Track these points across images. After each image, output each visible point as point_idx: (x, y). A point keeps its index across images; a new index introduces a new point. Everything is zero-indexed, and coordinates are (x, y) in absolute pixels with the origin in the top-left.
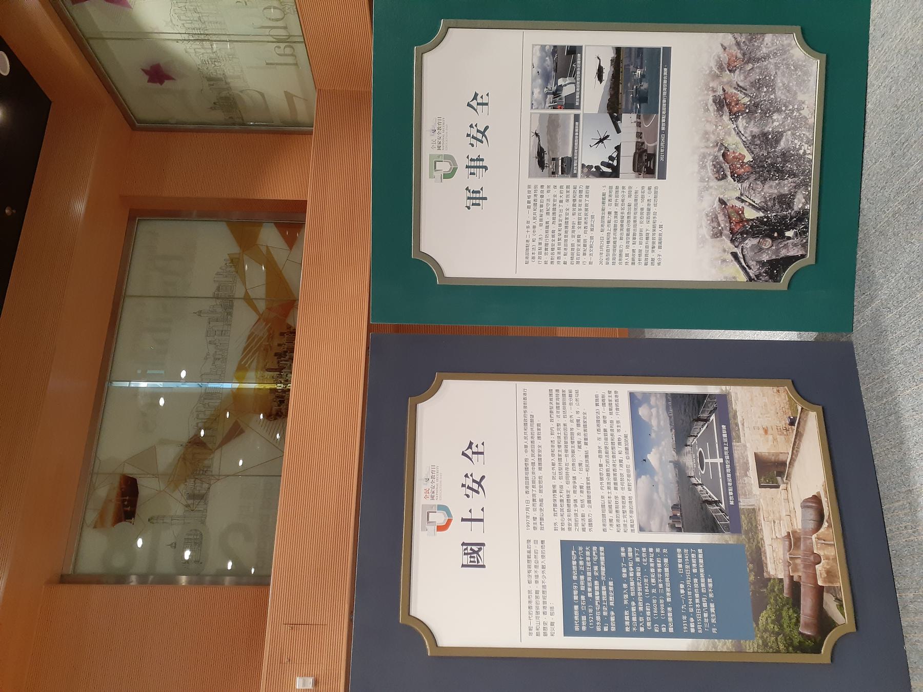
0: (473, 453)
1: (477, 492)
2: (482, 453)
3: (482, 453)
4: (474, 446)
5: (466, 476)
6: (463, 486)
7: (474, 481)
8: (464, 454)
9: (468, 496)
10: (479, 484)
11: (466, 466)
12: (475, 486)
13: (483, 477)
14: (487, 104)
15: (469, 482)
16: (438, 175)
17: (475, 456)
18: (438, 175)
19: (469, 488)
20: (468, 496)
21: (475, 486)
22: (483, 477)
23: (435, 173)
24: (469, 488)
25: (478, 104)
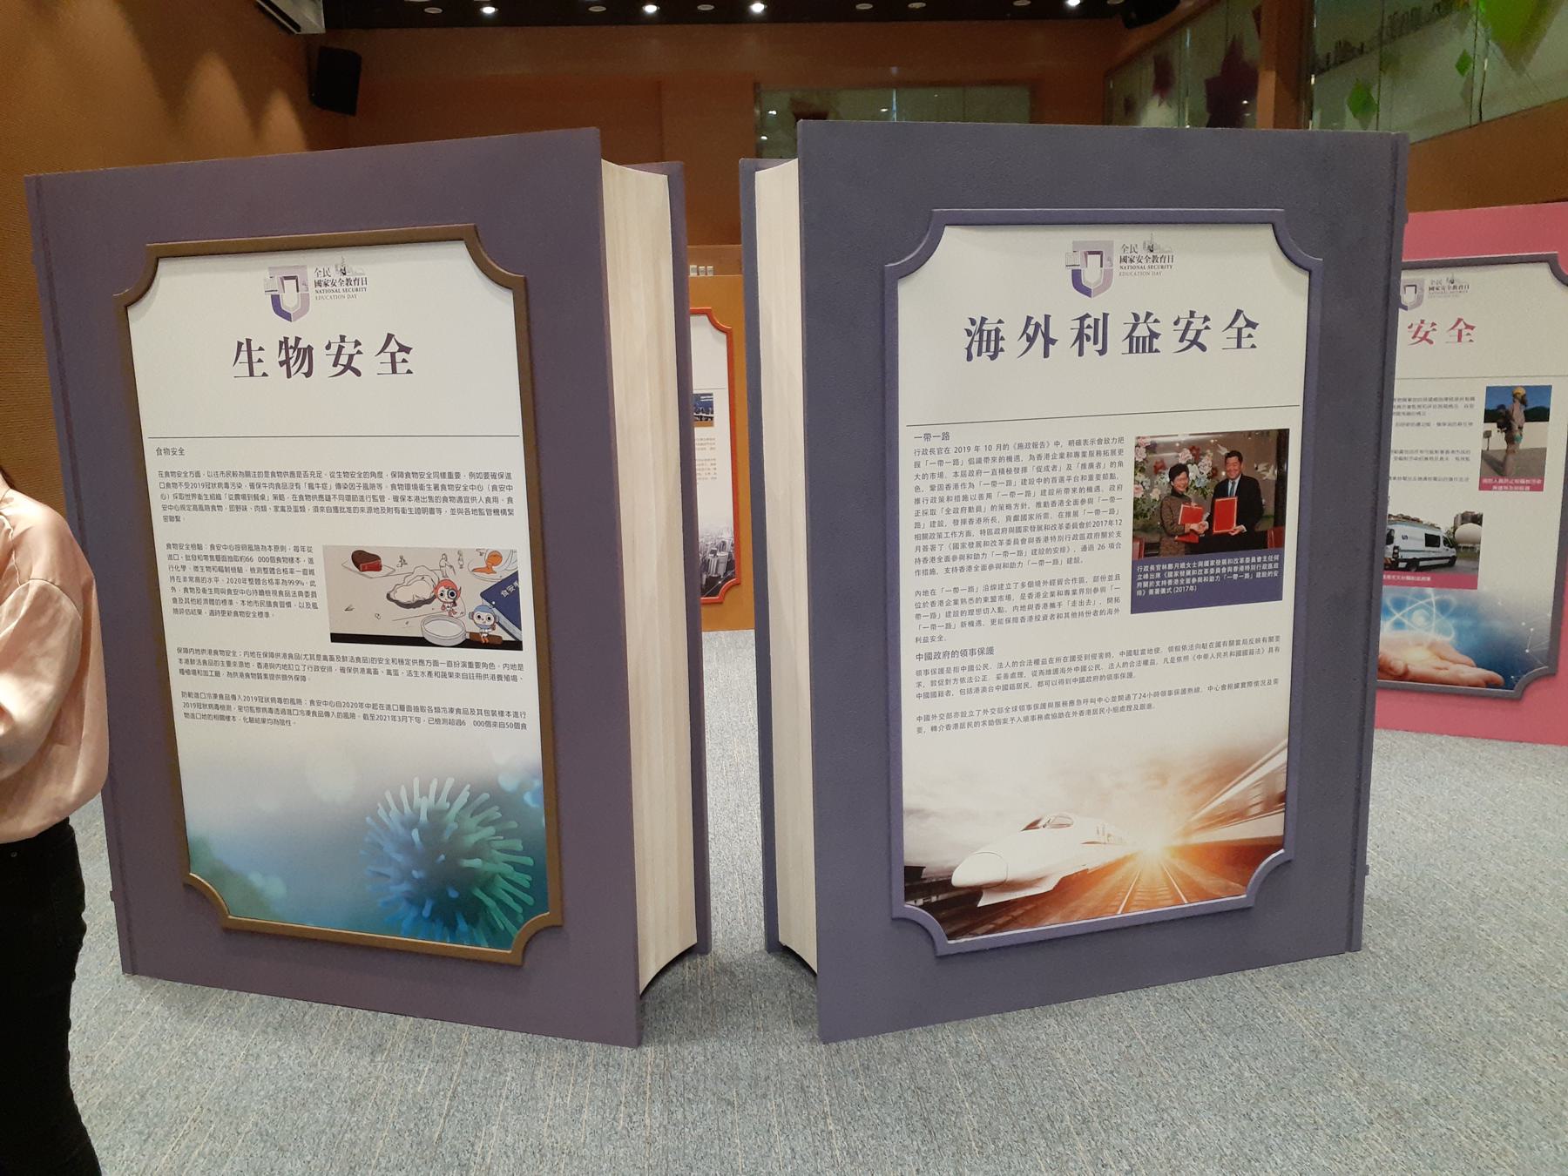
0: (1240, 330)
1: (1182, 340)
2: (1239, 346)
3: (1239, 346)
4: (1249, 330)
5: (1206, 319)
6: (1192, 314)
7: (1198, 332)
8: (1239, 313)
9: (1176, 323)
10: (1194, 342)
11: (1221, 318)
12: (1191, 335)
13: (1203, 348)
14: (394, 371)
15: (1197, 324)
16: (1078, 259)
17: (1233, 332)
18: (1078, 259)
19: (1189, 323)
20: (1176, 323)
21: (1191, 335)
22: (1203, 348)
23: (1079, 255)
24: (1189, 323)
25: (393, 355)
